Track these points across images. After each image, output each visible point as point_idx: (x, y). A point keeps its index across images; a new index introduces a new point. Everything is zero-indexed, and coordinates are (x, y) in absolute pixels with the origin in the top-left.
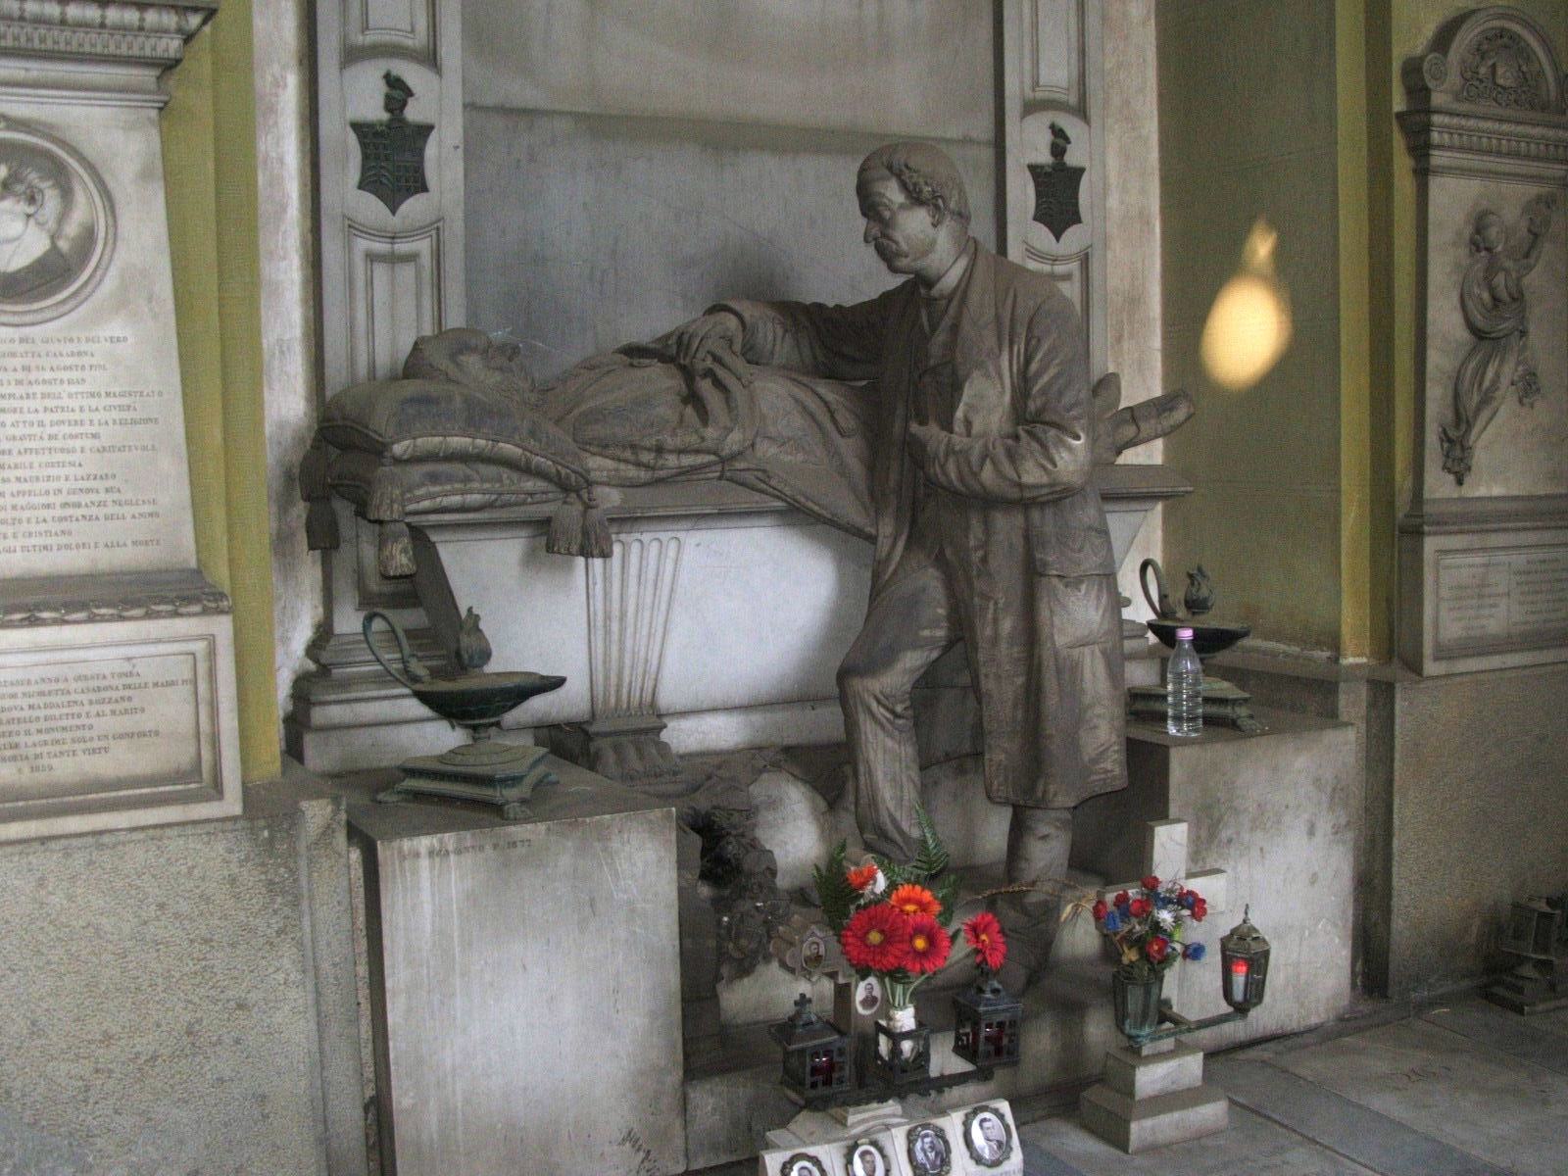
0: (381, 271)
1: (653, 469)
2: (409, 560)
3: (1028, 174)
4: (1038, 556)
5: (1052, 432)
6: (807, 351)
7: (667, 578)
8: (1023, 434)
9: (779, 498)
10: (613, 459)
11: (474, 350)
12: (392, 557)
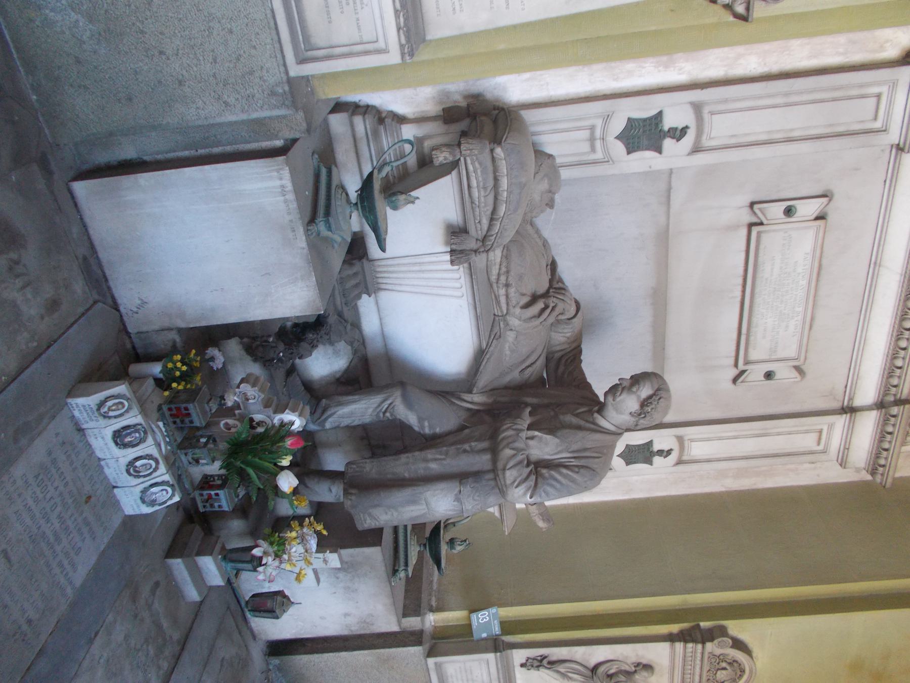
0: (586, 134)
1: (497, 283)
2: (441, 161)
4: (470, 480)
5: (533, 483)
6: (558, 348)
7: (442, 292)
8: (530, 469)
9: (487, 346)
10: (501, 262)
11: (551, 186)
12: (442, 152)
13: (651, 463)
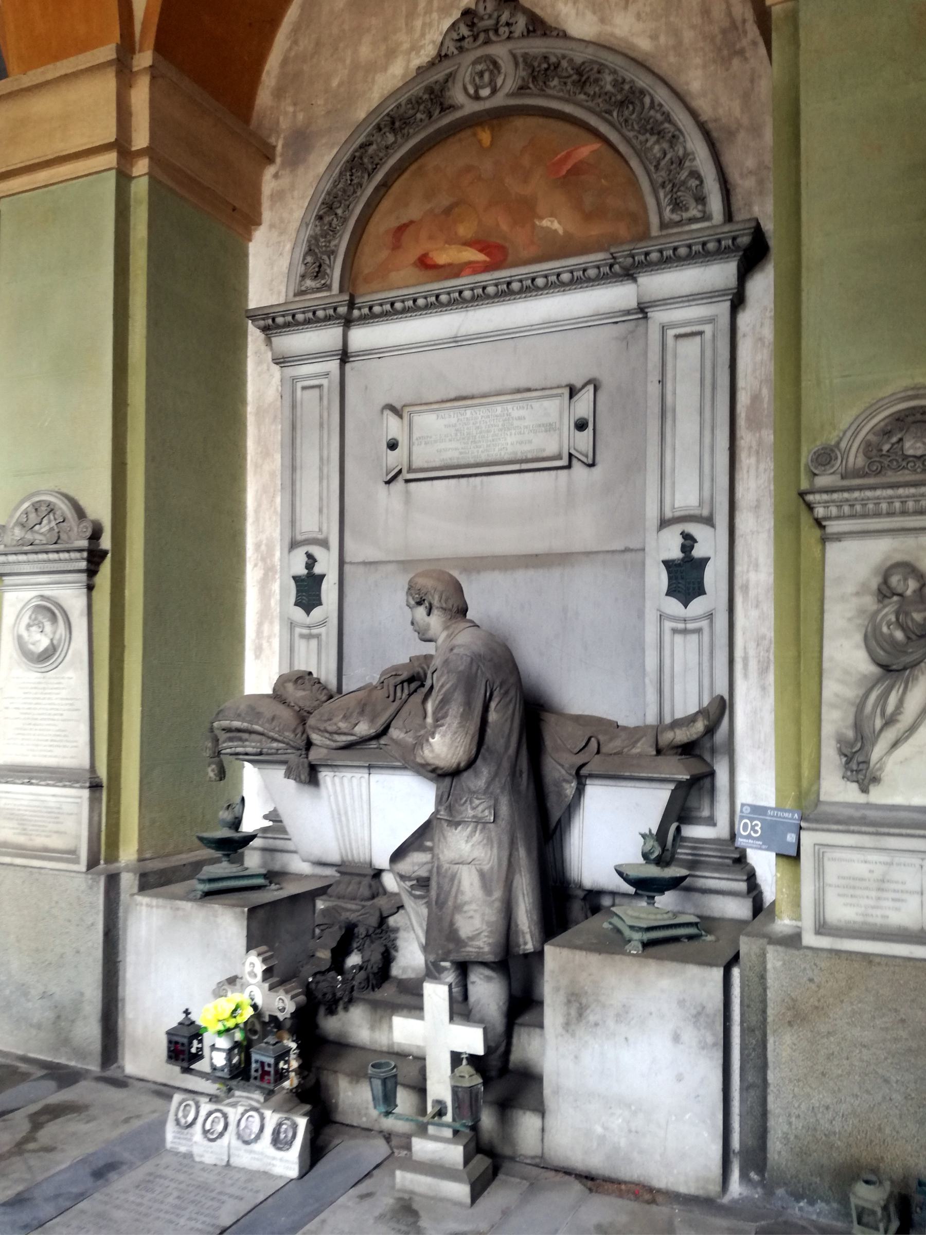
2: (215, 774)
3: (663, 567)
11: (290, 681)
13: (704, 561)
